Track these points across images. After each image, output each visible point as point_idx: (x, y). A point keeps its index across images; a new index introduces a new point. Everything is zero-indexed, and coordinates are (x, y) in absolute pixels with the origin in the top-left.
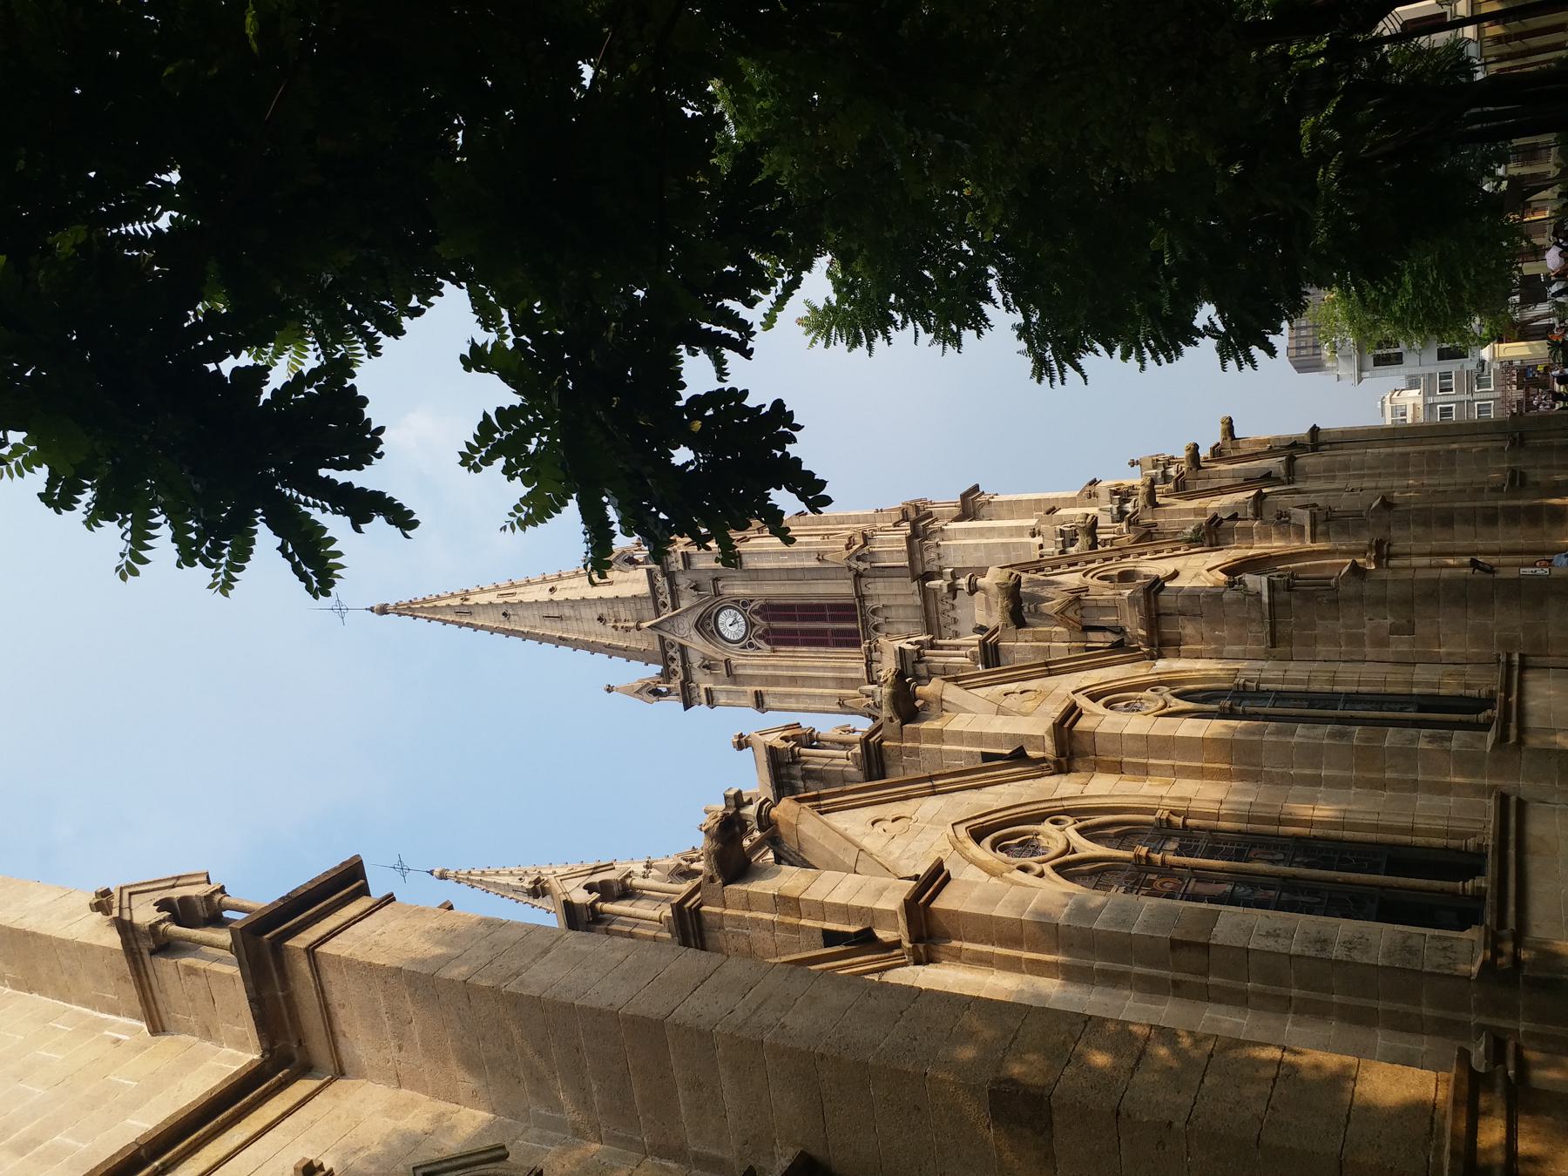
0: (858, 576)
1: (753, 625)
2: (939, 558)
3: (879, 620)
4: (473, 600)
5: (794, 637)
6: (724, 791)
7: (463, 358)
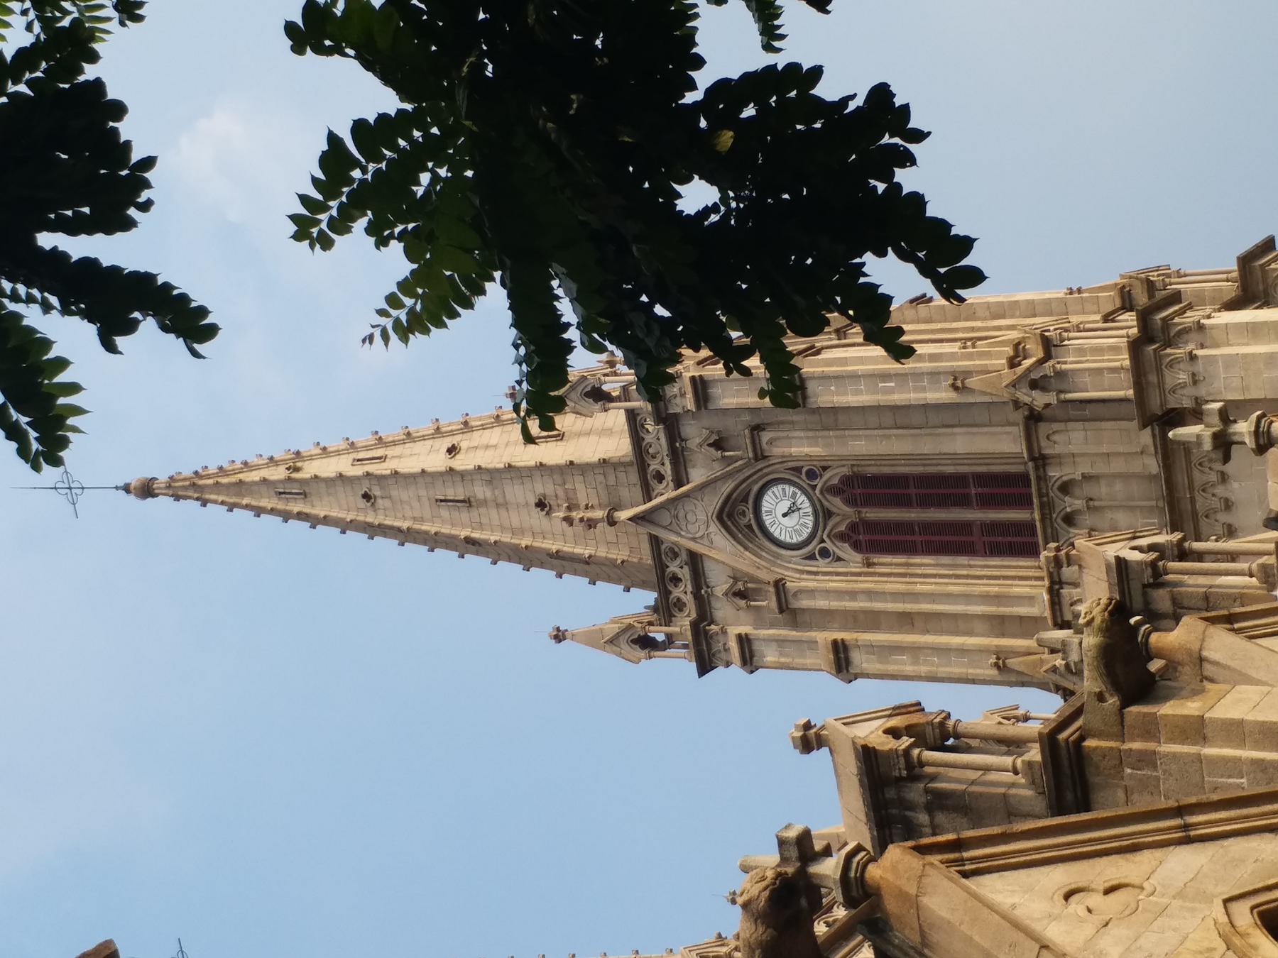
0: (1034, 418)
1: (828, 514)
2: (1195, 382)
3: (1073, 503)
4: (310, 469)
5: (909, 538)
6: (775, 832)
7: (290, 28)
